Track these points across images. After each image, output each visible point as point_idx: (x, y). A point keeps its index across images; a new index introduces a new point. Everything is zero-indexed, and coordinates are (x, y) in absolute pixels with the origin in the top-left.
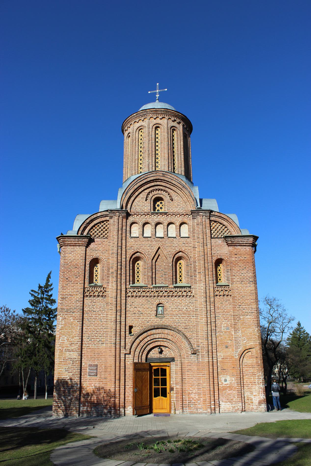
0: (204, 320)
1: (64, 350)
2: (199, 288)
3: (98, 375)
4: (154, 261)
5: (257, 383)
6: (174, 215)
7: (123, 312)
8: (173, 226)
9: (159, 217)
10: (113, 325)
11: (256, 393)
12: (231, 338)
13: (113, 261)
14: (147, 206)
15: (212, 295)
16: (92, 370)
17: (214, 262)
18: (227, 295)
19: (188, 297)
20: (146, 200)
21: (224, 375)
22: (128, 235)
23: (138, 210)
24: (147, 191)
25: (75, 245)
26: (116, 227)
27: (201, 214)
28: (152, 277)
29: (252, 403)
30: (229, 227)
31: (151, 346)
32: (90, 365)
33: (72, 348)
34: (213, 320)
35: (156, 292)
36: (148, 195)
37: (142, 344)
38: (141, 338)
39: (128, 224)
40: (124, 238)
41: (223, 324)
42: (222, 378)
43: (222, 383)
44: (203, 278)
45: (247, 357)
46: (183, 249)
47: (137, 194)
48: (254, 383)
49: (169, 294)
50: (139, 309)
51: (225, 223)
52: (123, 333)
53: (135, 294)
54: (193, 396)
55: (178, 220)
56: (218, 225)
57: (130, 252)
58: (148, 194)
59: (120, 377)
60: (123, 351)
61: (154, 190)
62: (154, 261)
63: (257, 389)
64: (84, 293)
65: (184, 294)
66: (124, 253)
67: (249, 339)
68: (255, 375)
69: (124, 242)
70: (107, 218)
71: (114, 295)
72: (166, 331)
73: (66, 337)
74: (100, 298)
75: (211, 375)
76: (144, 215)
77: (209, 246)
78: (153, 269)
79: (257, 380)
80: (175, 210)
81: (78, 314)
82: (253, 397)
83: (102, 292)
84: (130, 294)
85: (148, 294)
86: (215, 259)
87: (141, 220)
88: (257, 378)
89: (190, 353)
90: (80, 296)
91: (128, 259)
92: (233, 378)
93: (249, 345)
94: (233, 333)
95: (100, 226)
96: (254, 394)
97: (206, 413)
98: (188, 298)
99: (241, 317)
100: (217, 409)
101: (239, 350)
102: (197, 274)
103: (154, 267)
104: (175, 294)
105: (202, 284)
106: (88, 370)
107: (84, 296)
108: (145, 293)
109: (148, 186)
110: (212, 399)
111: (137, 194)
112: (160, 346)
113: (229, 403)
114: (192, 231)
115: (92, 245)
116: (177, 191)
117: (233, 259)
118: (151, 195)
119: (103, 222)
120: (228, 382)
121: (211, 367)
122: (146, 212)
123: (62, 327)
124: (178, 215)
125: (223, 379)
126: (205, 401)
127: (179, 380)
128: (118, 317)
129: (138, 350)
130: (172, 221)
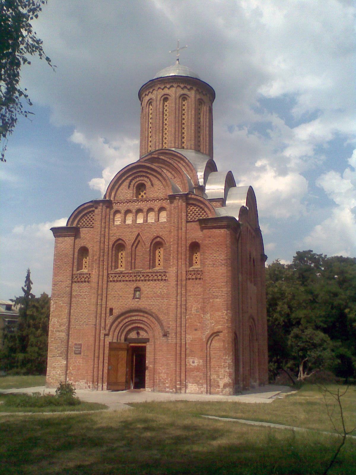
0: (174, 303)
1: (54, 331)
2: (172, 271)
3: (82, 354)
4: (134, 247)
5: (223, 367)
6: (154, 201)
7: (104, 295)
9: (140, 203)
10: (93, 308)
11: (223, 376)
12: (200, 321)
13: (96, 248)
15: (184, 278)
16: (77, 348)
17: (188, 245)
18: (200, 279)
19: (163, 280)
21: (193, 357)
22: (111, 223)
23: (122, 198)
24: (130, 178)
26: (100, 217)
27: (177, 198)
28: (131, 262)
29: (219, 386)
30: (206, 209)
31: (130, 327)
32: (76, 344)
33: (62, 329)
34: (184, 303)
35: (135, 276)
36: (131, 181)
37: (121, 325)
39: (112, 212)
40: (107, 227)
41: (194, 307)
42: (190, 360)
43: (190, 365)
44: (175, 262)
45: (216, 340)
46: (161, 234)
47: (120, 182)
48: (220, 366)
49: (146, 278)
50: (119, 292)
51: (202, 206)
52: (103, 315)
53: (115, 279)
54: (162, 375)
55: (157, 205)
56: (195, 208)
57: (113, 239)
58: (131, 181)
59: (99, 354)
60: (103, 332)
61: (137, 176)
62: (134, 247)
63: (222, 372)
64: (72, 279)
65: (160, 278)
66: (106, 240)
67: (217, 322)
68: (222, 358)
69: (107, 230)
70: (94, 209)
71: (96, 280)
72: (142, 314)
73: (56, 319)
74: (87, 283)
75: (178, 357)
76: (126, 203)
77: (184, 229)
78: (133, 255)
79: (223, 364)
80: (155, 195)
81: (66, 299)
82: (219, 380)
83: (87, 278)
84: (111, 279)
85: (127, 279)
86: (189, 242)
87: (123, 208)
88: (223, 361)
91: (111, 246)
92: (201, 361)
93: (217, 328)
94: (202, 316)
95: (88, 215)
96: (220, 377)
97: (171, 393)
98: (162, 282)
99: (211, 301)
100: (183, 389)
101: (207, 333)
102: (171, 257)
103: (133, 252)
104: (151, 278)
105: (174, 268)
106: (74, 349)
107: (72, 282)
108: (124, 277)
110: (178, 379)
111: (120, 182)
113: (195, 385)
114: (169, 216)
117: (206, 242)
118: (134, 182)
119: (90, 212)
120: (196, 364)
121: (178, 348)
122: (127, 200)
123: (53, 310)
124: (158, 201)
125: (191, 361)
126: (171, 380)
127: (152, 360)
128: (99, 301)
129: (117, 331)
130: (152, 206)
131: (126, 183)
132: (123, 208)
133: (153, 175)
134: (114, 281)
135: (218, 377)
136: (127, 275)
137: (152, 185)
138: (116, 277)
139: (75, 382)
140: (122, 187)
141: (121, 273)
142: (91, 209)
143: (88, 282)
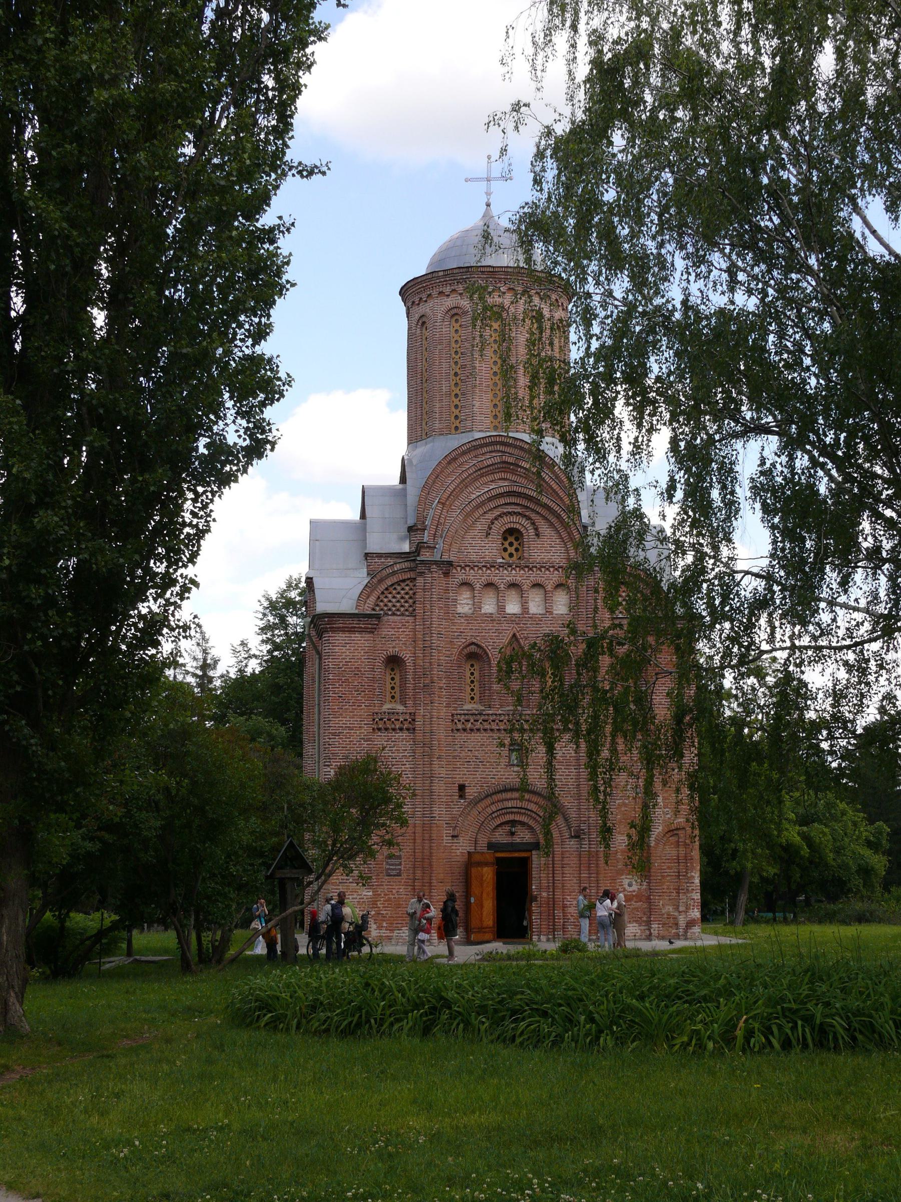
3: (404, 876)
8: (542, 591)
14: (489, 549)
20: (488, 534)
23: (474, 557)
25: (351, 630)
29: (677, 924)
38: (480, 807)
53: (469, 725)
57: (460, 642)
74: (405, 734)
84: (460, 726)
85: (494, 727)
89: (567, 835)
90: (366, 730)
95: (399, 588)
109: (492, 505)
112: (513, 823)
115: (385, 631)
116: (550, 517)
119: (404, 581)
130: (539, 580)
131: (481, 526)
132: (478, 578)
133: (538, 513)
134: (465, 730)
135: (677, 908)
136: (491, 718)
137: (537, 535)
138: (468, 721)
139: (392, 931)
140: (472, 533)
141: (480, 714)
142: (408, 576)
143: (408, 729)
